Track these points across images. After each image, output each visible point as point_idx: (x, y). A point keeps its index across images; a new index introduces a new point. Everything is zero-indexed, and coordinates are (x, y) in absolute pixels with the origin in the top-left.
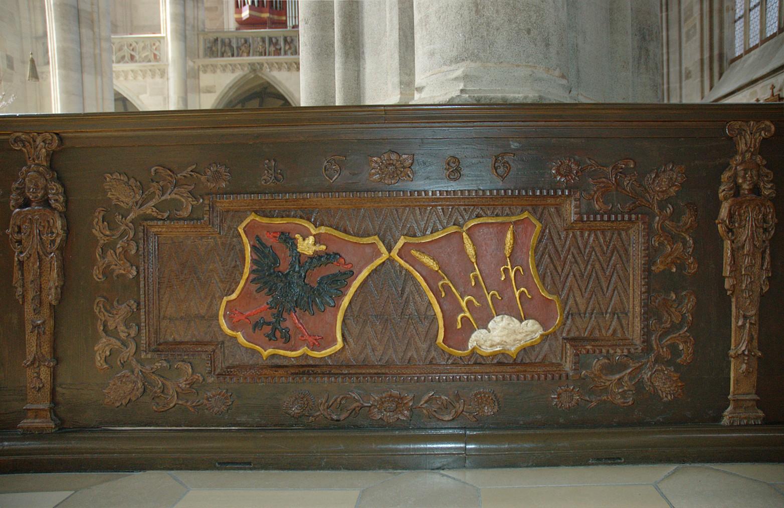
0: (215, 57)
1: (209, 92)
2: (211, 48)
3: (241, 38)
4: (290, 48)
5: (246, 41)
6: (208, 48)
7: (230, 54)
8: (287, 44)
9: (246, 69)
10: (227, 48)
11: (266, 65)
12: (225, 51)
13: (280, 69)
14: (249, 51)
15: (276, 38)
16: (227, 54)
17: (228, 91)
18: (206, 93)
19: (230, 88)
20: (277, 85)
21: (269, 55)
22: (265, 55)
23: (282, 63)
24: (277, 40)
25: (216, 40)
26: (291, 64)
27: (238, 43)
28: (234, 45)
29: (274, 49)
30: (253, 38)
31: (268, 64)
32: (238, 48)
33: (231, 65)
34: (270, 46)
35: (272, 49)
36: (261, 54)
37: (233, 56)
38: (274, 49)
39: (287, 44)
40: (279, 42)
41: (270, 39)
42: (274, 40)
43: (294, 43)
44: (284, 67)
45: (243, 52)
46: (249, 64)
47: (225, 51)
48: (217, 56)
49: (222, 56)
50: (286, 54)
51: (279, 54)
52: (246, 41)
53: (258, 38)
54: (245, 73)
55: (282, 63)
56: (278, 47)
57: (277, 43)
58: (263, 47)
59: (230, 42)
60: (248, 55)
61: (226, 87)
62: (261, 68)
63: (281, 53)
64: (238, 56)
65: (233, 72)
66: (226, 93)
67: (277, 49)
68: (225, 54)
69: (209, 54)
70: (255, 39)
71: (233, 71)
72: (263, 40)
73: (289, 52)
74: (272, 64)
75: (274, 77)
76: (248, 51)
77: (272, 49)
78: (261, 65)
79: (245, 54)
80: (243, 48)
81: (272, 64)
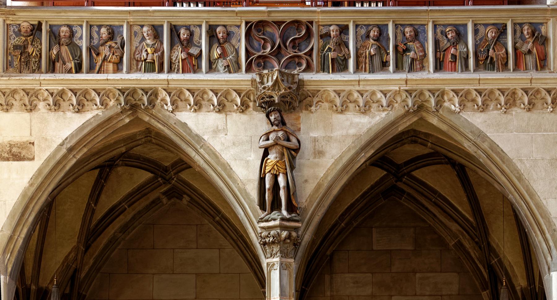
0: (33, 72)
1: (17, 157)
2: (22, 49)
3: (100, 27)
4: (223, 55)
5: (112, 35)
6: (16, 47)
7: (71, 65)
8: (216, 45)
9: (112, 103)
10: (65, 50)
11: (163, 94)
12: (58, 55)
13: (198, 106)
14: (121, 58)
15: (188, 28)
16: (64, 63)
17: (65, 157)
18: (8, 159)
19: (70, 150)
20: (188, 143)
21: (170, 70)
22: (161, 70)
23: (204, 92)
24: (191, 34)
25: (37, 29)
26: (226, 94)
27: (91, 38)
28: (84, 44)
29: (183, 56)
30: (130, 27)
31: (169, 94)
32: (93, 50)
33: (73, 91)
34: (172, 45)
35: (179, 54)
36: (150, 67)
37: (78, 69)
38: (183, 56)
39: (216, 45)
40: (196, 38)
41: (174, 30)
42: (184, 35)
43: (234, 41)
44: (210, 100)
45: (105, 60)
46: (122, 91)
47: (58, 55)
48: (38, 70)
49: (52, 68)
50: (211, 68)
51: (196, 69)
52: (113, 33)
53: (142, 26)
54: (110, 113)
55: (204, 92)
56: (194, 51)
57: (190, 41)
58: (155, 51)
59: (72, 34)
60: (118, 68)
61: (62, 145)
62: (151, 103)
63: (199, 67)
64: (91, 69)
65: (79, 111)
66: (59, 163)
67: (190, 55)
68: (58, 65)
69: (16, 63)
70: (136, 28)
71: (80, 108)
72: (157, 32)
73: (221, 64)
74: (180, 93)
75: (185, 125)
76: (115, 59)
77: (179, 54)
78: (153, 94)
79: (111, 66)
80: (105, 51)
81: (180, 93)
